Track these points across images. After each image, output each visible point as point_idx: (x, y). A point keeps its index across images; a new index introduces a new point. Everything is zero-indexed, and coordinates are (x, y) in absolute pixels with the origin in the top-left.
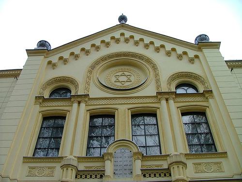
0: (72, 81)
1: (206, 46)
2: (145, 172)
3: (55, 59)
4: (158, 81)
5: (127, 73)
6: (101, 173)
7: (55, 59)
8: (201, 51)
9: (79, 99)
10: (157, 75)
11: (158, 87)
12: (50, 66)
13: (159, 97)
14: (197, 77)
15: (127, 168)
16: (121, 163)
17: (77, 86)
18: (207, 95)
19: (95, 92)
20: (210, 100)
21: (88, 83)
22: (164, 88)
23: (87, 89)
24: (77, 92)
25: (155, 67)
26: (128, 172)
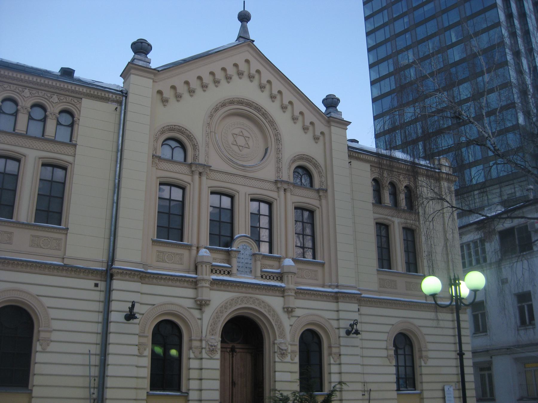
0: (190, 137)
1: (337, 122)
2: (263, 274)
3: (165, 86)
4: (279, 160)
5: (246, 134)
6: (229, 270)
7: (165, 86)
8: (329, 127)
9: (201, 170)
10: (279, 151)
11: (279, 170)
12: (159, 97)
13: (279, 185)
14: (316, 165)
15: (248, 266)
16: (243, 261)
17: (195, 147)
18: (321, 194)
19: (216, 162)
20: (324, 202)
21: (207, 145)
22: (285, 178)
23: (207, 155)
24: (195, 157)
25: (278, 140)
26: (248, 270)
